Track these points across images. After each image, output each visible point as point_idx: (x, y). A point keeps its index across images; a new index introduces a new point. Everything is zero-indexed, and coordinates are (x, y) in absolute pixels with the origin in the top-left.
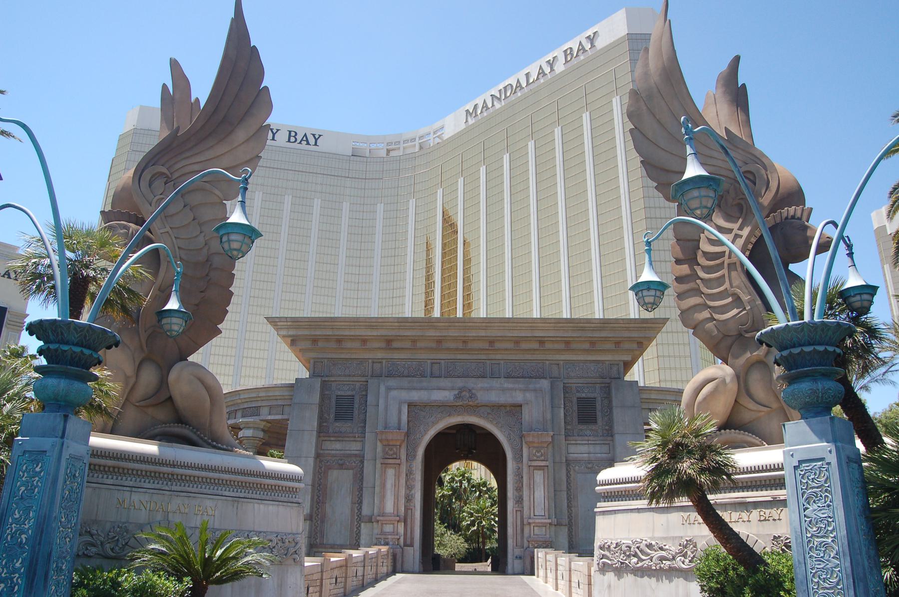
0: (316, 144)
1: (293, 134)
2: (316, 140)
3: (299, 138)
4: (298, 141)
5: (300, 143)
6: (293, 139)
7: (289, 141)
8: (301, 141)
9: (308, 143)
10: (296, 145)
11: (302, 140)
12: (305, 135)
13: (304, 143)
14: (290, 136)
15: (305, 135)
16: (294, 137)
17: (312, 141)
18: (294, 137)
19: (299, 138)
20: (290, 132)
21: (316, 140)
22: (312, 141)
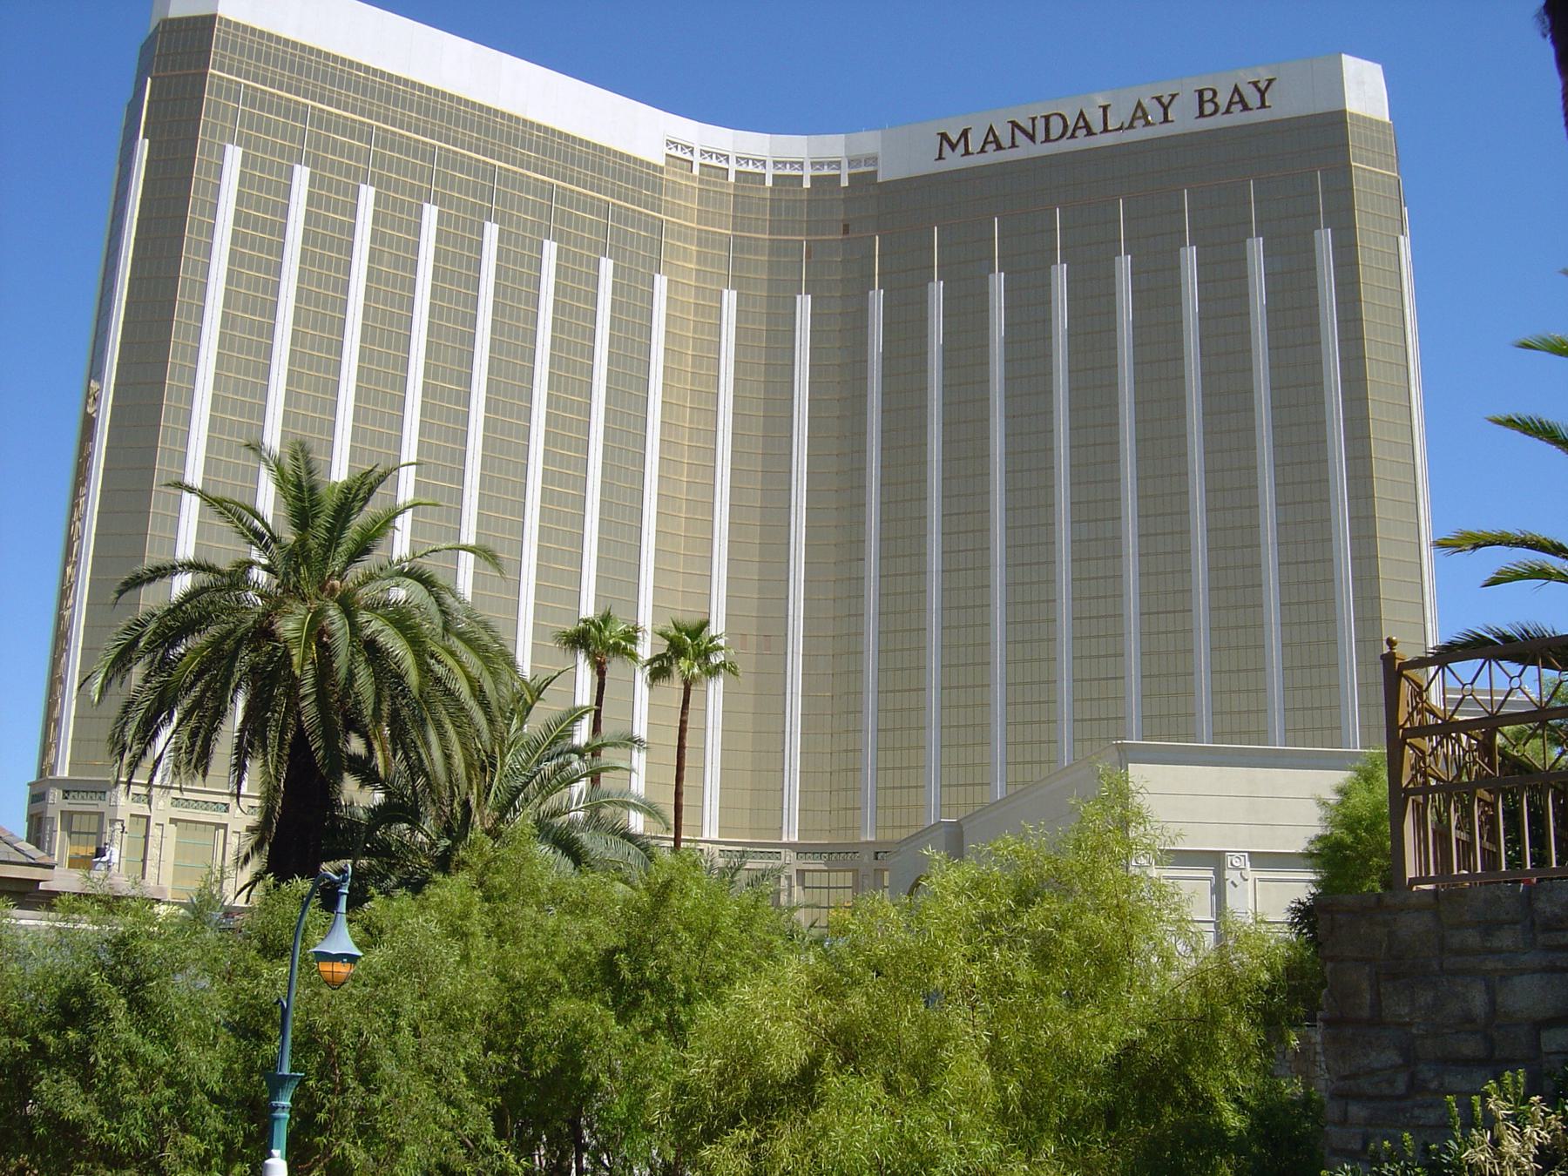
0: (1263, 105)
1: (1208, 95)
2: (1262, 94)
4: (1223, 109)
5: (1228, 111)
6: (1209, 108)
7: (1202, 115)
9: (1246, 108)
11: (1231, 103)
12: (1236, 89)
13: (1237, 108)
14: (1201, 102)
15: (1236, 89)
16: (1211, 100)
17: (1253, 98)
18: (1211, 100)
19: (1223, 100)
20: (1201, 93)
21: (1262, 94)
22: (1253, 98)
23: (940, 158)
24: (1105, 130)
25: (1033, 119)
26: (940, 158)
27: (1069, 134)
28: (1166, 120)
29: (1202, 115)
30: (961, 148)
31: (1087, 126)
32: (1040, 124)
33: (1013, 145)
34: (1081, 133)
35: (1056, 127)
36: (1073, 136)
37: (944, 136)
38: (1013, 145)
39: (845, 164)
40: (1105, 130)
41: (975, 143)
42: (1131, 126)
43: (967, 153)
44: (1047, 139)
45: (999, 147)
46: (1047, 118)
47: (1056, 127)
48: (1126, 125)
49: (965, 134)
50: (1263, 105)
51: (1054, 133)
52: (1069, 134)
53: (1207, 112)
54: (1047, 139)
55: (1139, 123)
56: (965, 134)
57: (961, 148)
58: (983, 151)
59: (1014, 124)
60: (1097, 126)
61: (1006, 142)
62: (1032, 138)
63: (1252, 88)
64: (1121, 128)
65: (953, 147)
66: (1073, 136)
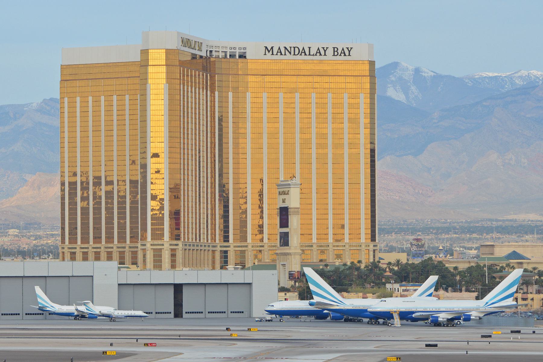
0: (349, 55)
1: (336, 50)
3: (339, 52)
4: (339, 54)
6: (336, 53)
7: (334, 55)
8: (341, 54)
10: (338, 58)
11: (341, 53)
12: (343, 49)
13: (343, 55)
15: (343, 49)
18: (337, 51)
19: (339, 52)
20: (334, 48)
22: (347, 53)
23: (265, 54)
24: (309, 55)
25: (291, 47)
26: (265, 54)
27: (300, 54)
28: (325, 55)
29: (334, 55)
30: (271, 51)
31: (305, 52)
32: (293, 49)
33: (285, 55)
34: (303, 54)
35: (297, 53)
36: (301, 55)
37: (266, 48)
38: (285, 55)
39: (237, 49)
40: (309, 55)
41: (275, 53)
42: (316, 55)
43: (273, 54)
44: (294, 54)
45: (281, 54)
46: (294, 48)
47: (296, 53)
48: (315, 54)
49: (272, 48)
50: (349, 55)
51: (296, 53)
52: (300, 54)
53: (335, 55)
54: (294, 54)
55: (318, 54)
56: (272, 48)
57: (271, 52)
58: (277, 54)
59: (285, 48)
60: (307, 53)
61: (283, 53)
62: (290, 53)
63: (347, 49)
64: (313, 55)
65: (269, 51)
66: (301, 55)
